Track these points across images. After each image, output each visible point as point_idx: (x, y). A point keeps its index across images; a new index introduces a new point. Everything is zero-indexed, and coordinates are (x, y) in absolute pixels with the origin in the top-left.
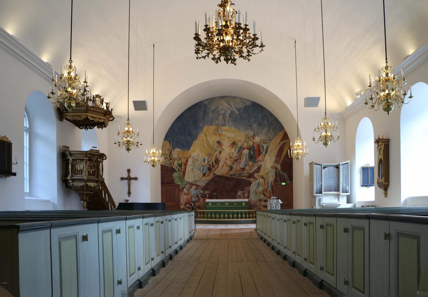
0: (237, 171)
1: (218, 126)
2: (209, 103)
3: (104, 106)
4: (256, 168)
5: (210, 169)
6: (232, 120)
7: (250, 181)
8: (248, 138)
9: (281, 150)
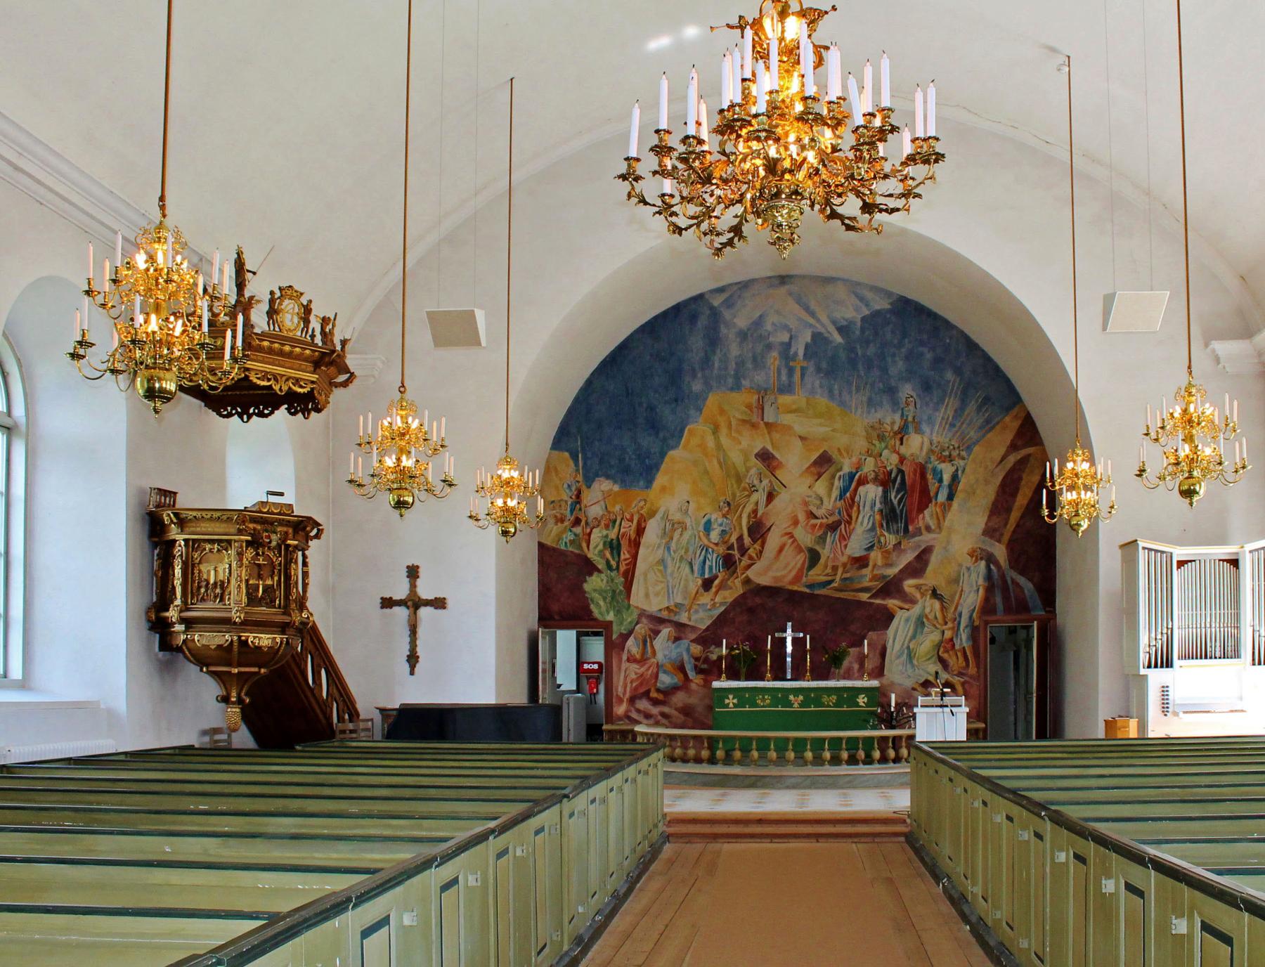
0: (835, 568)
2: (729, 303)
4: (908, 557)
5: (729, 562)
6: (819, 370)
7: (885, 608)
9: (1009, 487)
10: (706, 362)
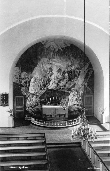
1: (50, 58)
4: (72, 85)
5: (45, 86)
6: (59, 54)
7: (69, 93)
8: (68, 66)
9: (88, 74)
10: (41, 53)
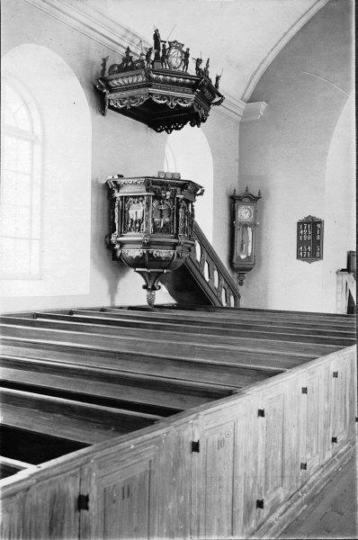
3: (192, 70)
